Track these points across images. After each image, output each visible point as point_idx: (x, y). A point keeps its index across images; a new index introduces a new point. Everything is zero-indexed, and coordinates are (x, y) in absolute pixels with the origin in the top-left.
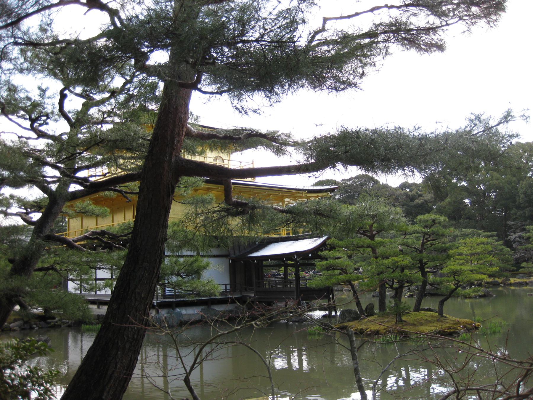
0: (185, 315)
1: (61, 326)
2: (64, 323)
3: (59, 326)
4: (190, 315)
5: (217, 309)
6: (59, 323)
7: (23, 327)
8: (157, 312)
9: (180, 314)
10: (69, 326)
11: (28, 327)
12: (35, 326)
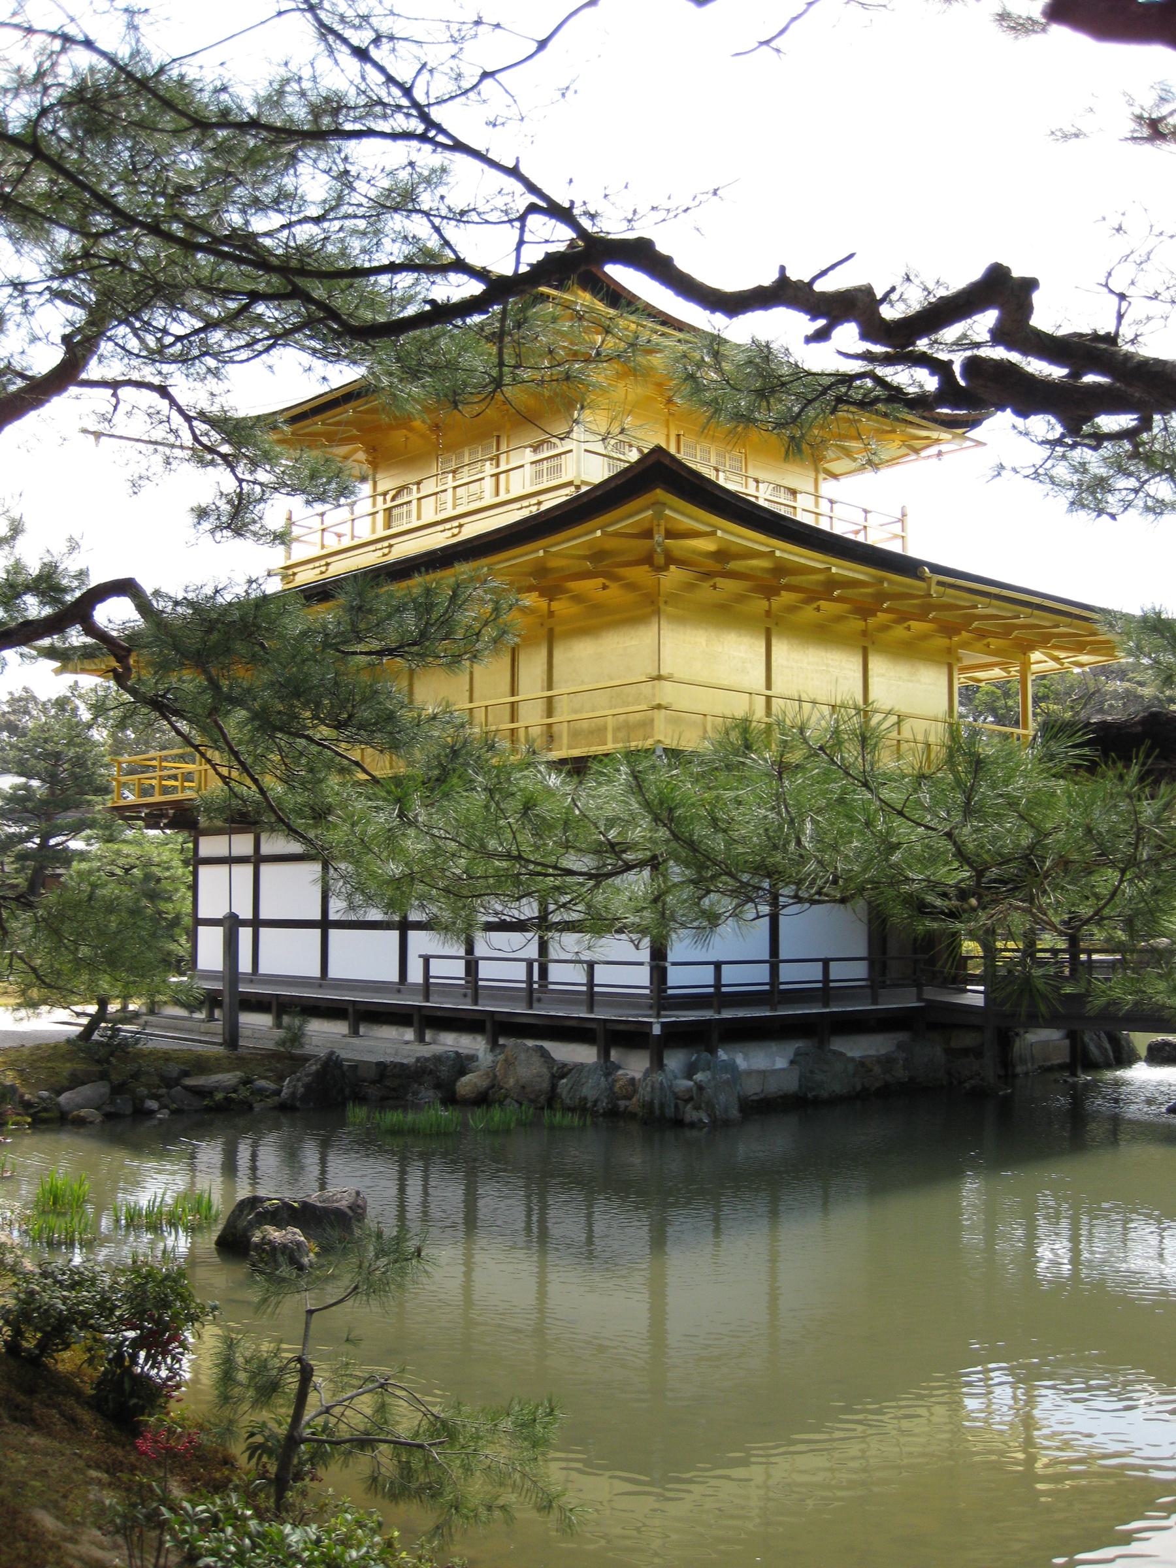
0: (749, 1073)
1: (251, 1108)
2: (261, 1091)
3: (246, 1107)
4: (762, 1073)
5: (849, 1054)
6: (244, 1093)
7: (108, 1109)
8: (658, 1063)
9: (731, 1067)
10: (285, 1108)
11: (128, 1110)
12: (153, 1104)
